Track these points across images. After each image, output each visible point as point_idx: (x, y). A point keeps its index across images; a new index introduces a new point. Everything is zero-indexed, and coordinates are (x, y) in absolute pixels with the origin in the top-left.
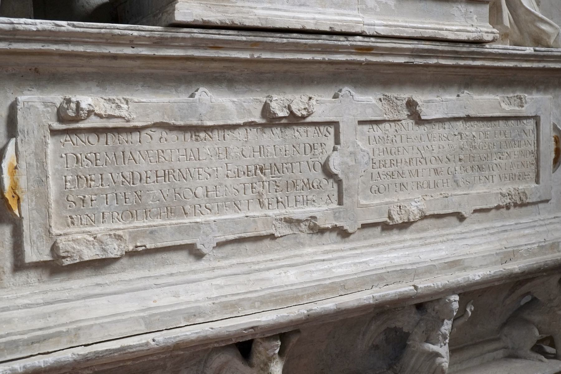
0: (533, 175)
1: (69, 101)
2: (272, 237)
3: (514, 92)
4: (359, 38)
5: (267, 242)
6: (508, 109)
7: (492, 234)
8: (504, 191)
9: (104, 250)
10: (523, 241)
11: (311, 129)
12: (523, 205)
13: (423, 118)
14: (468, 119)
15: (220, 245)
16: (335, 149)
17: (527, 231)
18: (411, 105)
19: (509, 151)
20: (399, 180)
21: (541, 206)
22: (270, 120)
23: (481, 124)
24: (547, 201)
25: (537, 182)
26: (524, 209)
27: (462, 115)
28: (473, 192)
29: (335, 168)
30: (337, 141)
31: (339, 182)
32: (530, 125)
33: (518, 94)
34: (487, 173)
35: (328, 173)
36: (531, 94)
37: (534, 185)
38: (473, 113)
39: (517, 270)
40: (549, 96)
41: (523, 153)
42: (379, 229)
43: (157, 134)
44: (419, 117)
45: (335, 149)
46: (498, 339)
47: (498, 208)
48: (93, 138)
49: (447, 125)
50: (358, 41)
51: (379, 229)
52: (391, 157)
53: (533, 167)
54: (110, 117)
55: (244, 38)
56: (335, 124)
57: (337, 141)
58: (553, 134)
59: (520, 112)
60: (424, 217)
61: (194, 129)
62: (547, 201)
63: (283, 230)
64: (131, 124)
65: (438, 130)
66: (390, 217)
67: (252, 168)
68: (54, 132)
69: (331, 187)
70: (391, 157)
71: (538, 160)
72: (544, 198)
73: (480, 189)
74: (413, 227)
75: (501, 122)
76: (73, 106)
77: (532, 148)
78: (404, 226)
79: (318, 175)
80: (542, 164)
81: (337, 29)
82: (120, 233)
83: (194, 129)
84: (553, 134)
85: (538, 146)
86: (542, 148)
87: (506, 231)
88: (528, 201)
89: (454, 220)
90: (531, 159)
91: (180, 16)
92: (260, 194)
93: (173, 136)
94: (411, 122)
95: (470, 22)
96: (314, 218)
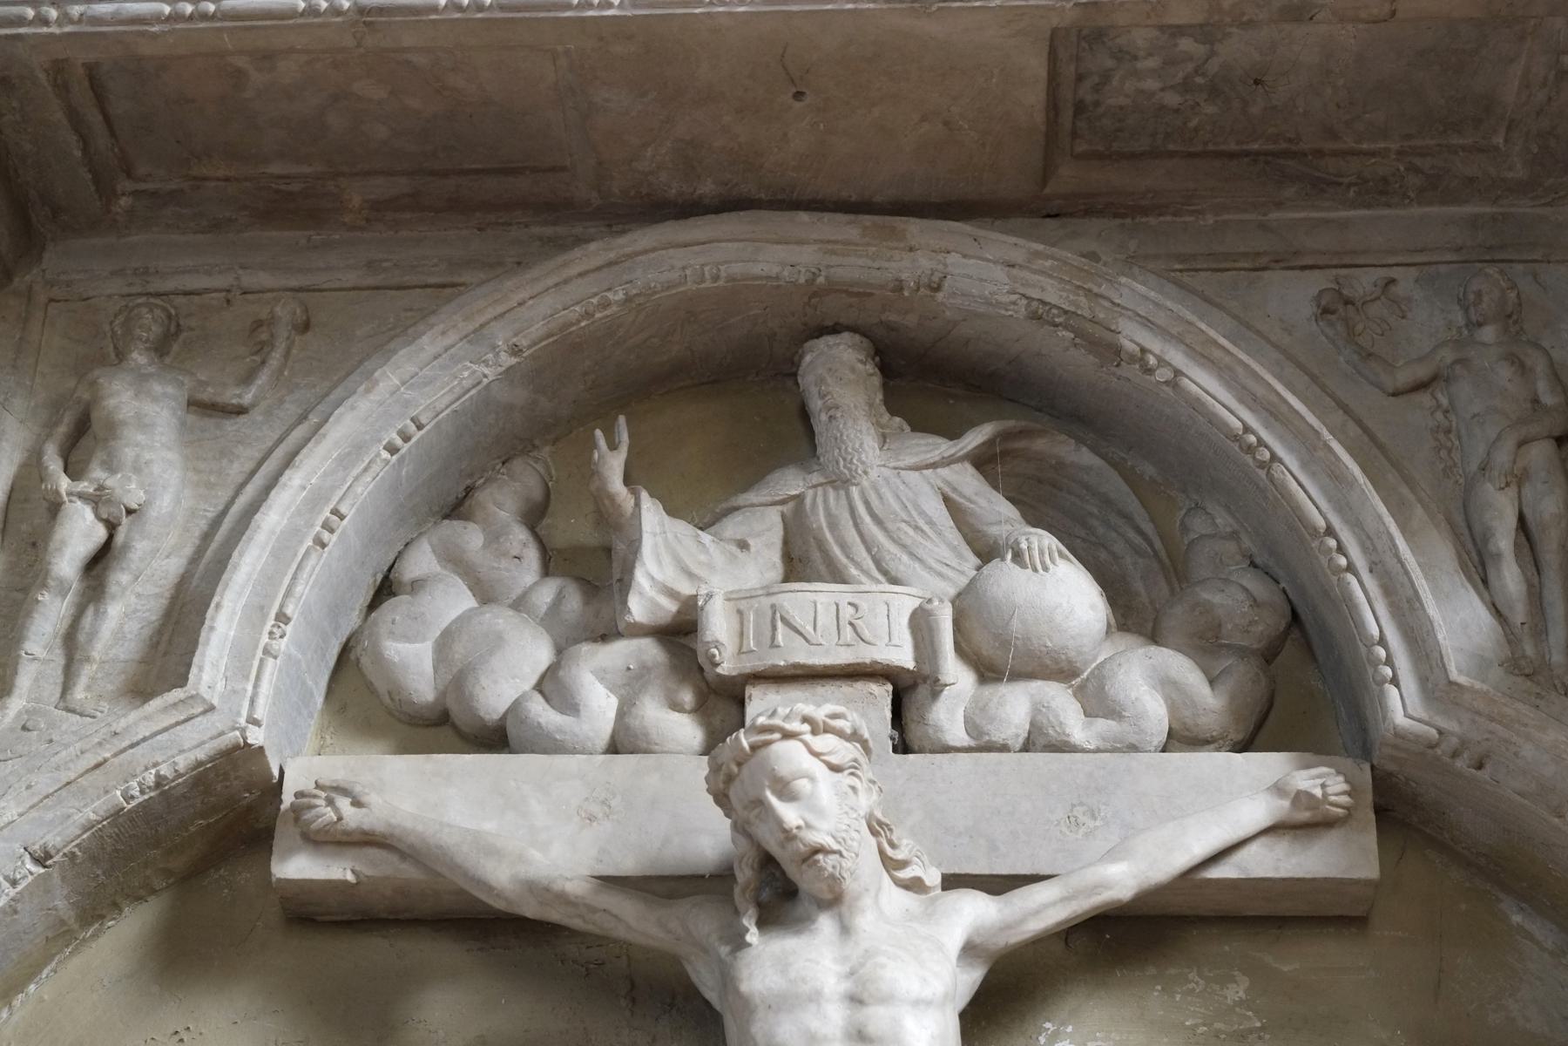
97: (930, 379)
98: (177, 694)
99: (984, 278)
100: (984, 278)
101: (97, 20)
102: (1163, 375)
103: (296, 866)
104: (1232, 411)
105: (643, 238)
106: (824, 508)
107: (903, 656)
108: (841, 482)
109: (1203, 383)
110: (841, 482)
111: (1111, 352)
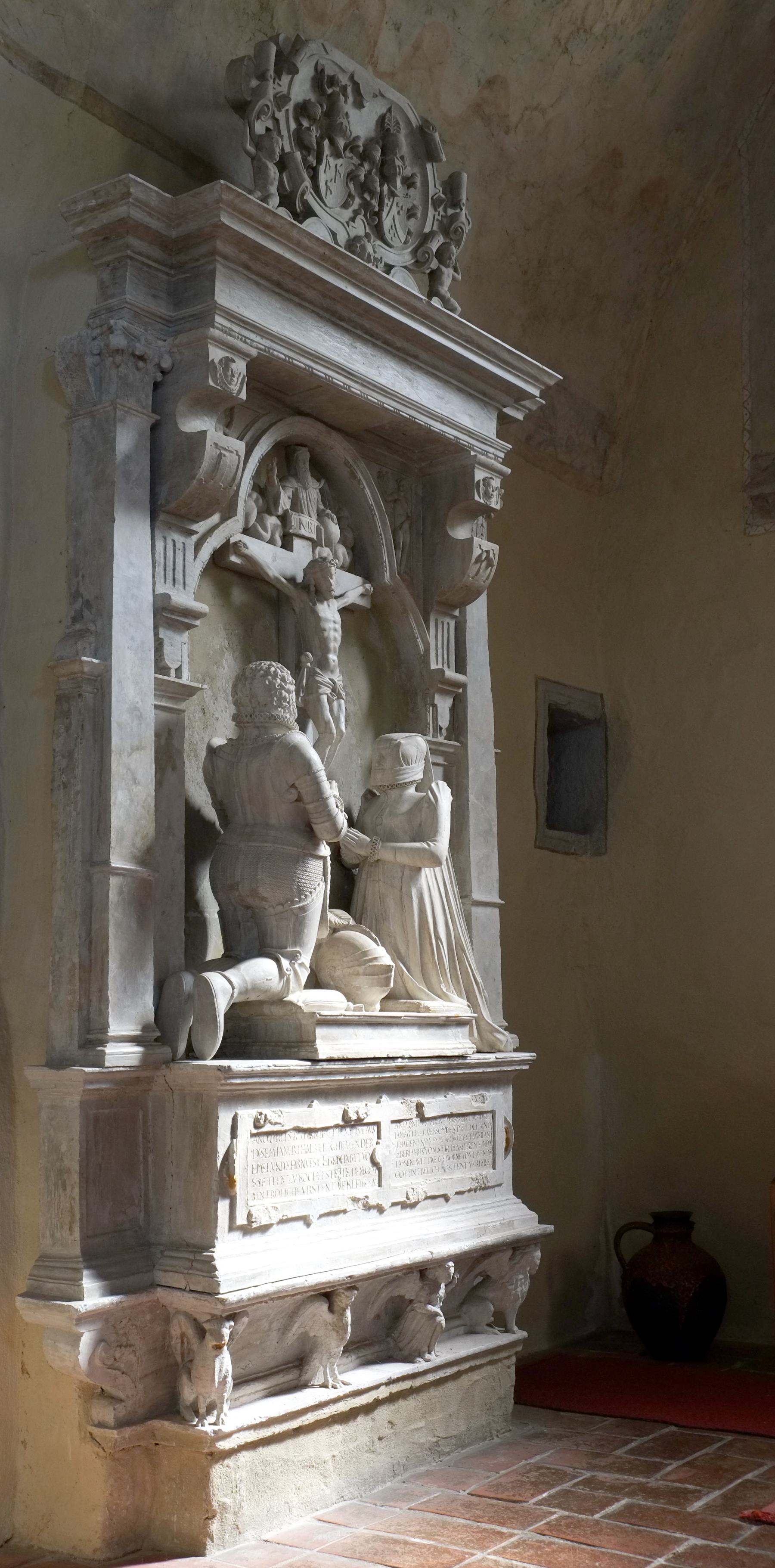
0: (491, 1162)
1: (261, 1114)
2: (344, 1212)
3: (478, 1091)
4: (400, 1060)
5: (342, 1215)
6: (476, 1106)
7: (468, 1213)
8: (474, 1176)
9: (270, 1217)
10: (489, 1219)
11: (365, 1128)
12: (486, 1188)
13: (426, 1116)
14: (451, 1115)
15: (321, 1216)
16: (378, 1143)
17: (490, 1211)
18: (419, 1107)
19: (475, 1141)
20: (411, 1167)
21: (496, 1189)
22: (348, 1123)
23: (458, 1119)
24: (500, 1185)
25: (494, 1168)
26: (485, 1191)
27: (448, 1113)
28: (454, 1177)
29: (379, 1158)
30: (379, 1137)
31: (379, 1169)
32: (488, 1118)
33: (481, 1092)
34: (461, 1161)
35: (374, 1163)
36: (488, 1091)
37: (492, 1171)
38: (455, 1111)
39: (490, 1243)
40: (501, 1093)
41: (484, 1143)
42: (400, 1207)
43: (293, 1134)
44: (423, 1115)
45: (378, 1143)
46: (459, 1317)
47: (469, 1191)
48: (265, 1138)
49: (438, 1121)
50: (399, 1062)
51: (400, 1207)
52: (407, 1148)
53: (491, 1155)
54: (276, 1124)
55: (345, 1066)
56: (378, 1124)
57: (379, 1137)
58: (504, 1126)
59: (483, 1107)
60: (427, 1198)
61: (309, 1131)
62: (500, 1185)
63: (350, 1206)
64: (283, 1129)
65: (432, 1125)
66: (408, 1198)
67: (335, 1159)
68: (253, 1135)
69: (374, 1172)
70: (407, 1148)
71: (494, 1148)
72: (499, 1183)
73: (458, 1175)
74: (418, 1206)
75: (471, 1117)
76: (263, 1117)
77: (490, 1138)
78: (413, 1206)
79: (368, 1163)
80: (497, 1151)
81: (391, 1056)
82: (276, 1205)
83: (309, 1131)
84: (504, 1126)
85: (494, 1136)
86: (497, 1138)
87: (476, 1210)
88: (489, 1184)
89: (442, 1200)
90: (489, 1147)
91: (322, 1056)
92: (339, 1178)
93: (301, 1135)
94: (418, 1120)
95: (459, 1041)
96: (367, 1197)
97: (320, 469)
98: (235, 518)
99: (340, 451)
100: (340, 451)
101: (273, 355)
102: (361, 486)
103: (234, 559)
104: (371, 502)
105: (297, 418)
106: (303, 495)
107: (314, 536)
108: (305, 488)
109: (368, 491)
110: (305, 488)
111: (353, 476)
